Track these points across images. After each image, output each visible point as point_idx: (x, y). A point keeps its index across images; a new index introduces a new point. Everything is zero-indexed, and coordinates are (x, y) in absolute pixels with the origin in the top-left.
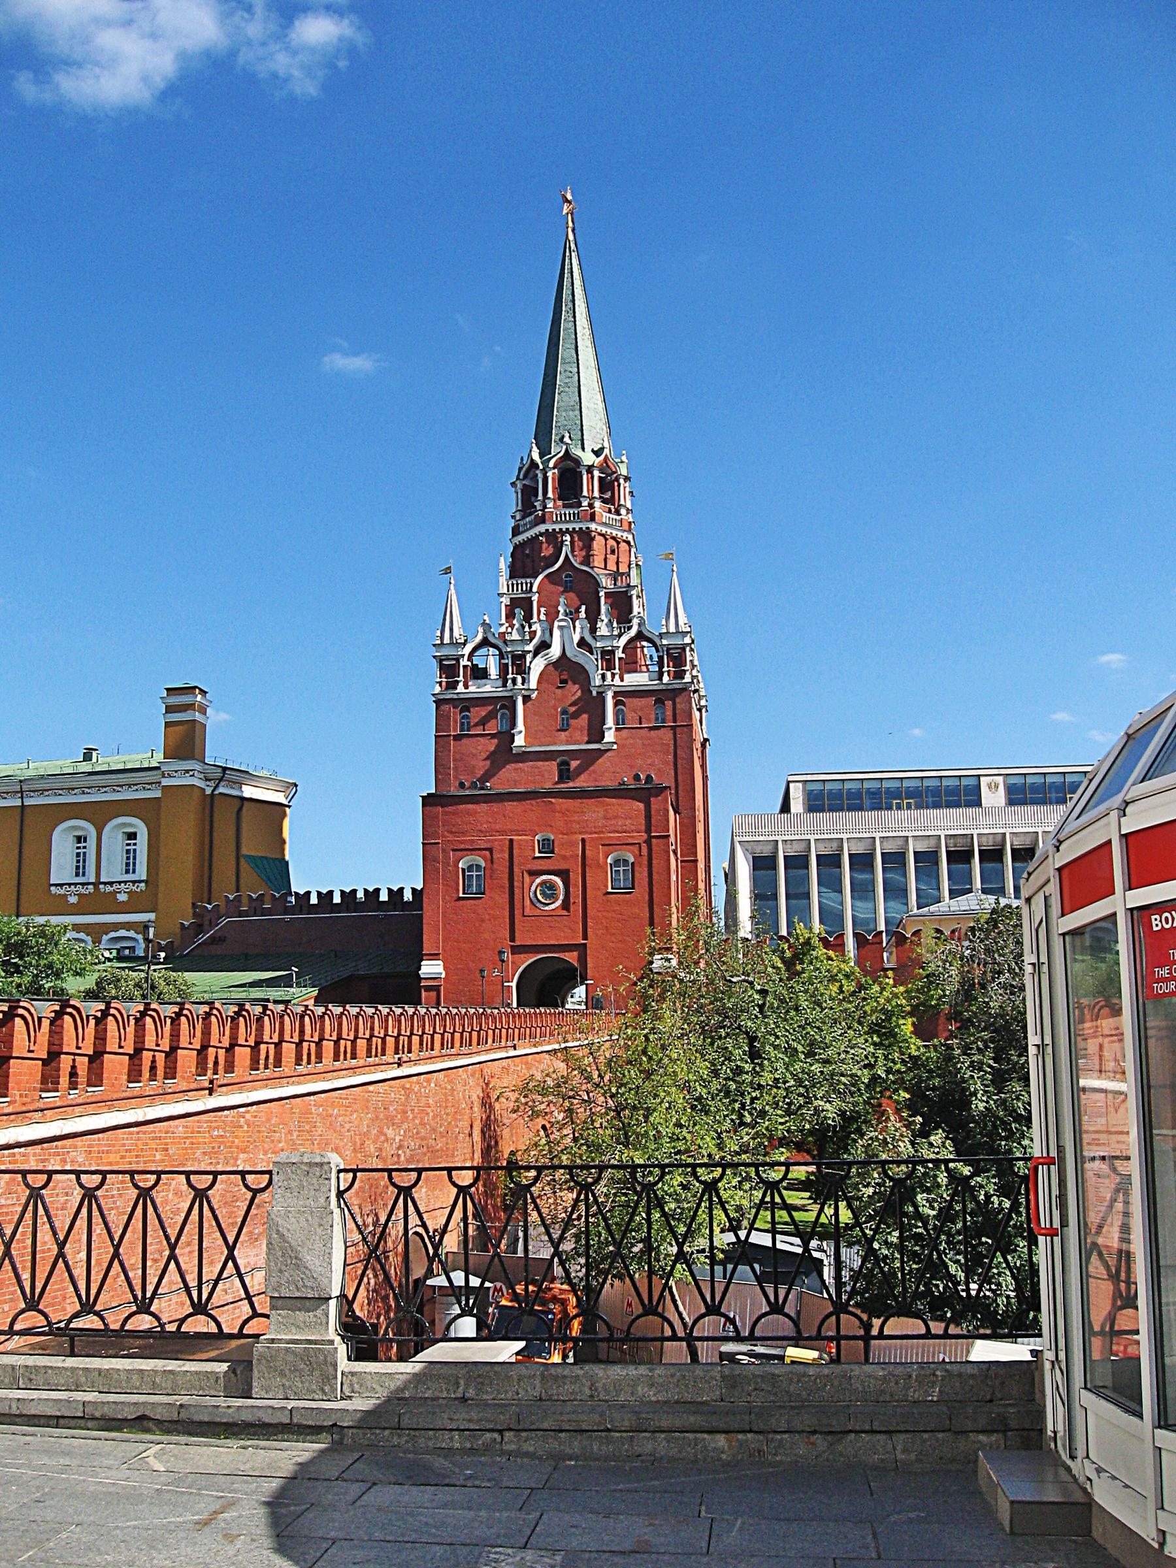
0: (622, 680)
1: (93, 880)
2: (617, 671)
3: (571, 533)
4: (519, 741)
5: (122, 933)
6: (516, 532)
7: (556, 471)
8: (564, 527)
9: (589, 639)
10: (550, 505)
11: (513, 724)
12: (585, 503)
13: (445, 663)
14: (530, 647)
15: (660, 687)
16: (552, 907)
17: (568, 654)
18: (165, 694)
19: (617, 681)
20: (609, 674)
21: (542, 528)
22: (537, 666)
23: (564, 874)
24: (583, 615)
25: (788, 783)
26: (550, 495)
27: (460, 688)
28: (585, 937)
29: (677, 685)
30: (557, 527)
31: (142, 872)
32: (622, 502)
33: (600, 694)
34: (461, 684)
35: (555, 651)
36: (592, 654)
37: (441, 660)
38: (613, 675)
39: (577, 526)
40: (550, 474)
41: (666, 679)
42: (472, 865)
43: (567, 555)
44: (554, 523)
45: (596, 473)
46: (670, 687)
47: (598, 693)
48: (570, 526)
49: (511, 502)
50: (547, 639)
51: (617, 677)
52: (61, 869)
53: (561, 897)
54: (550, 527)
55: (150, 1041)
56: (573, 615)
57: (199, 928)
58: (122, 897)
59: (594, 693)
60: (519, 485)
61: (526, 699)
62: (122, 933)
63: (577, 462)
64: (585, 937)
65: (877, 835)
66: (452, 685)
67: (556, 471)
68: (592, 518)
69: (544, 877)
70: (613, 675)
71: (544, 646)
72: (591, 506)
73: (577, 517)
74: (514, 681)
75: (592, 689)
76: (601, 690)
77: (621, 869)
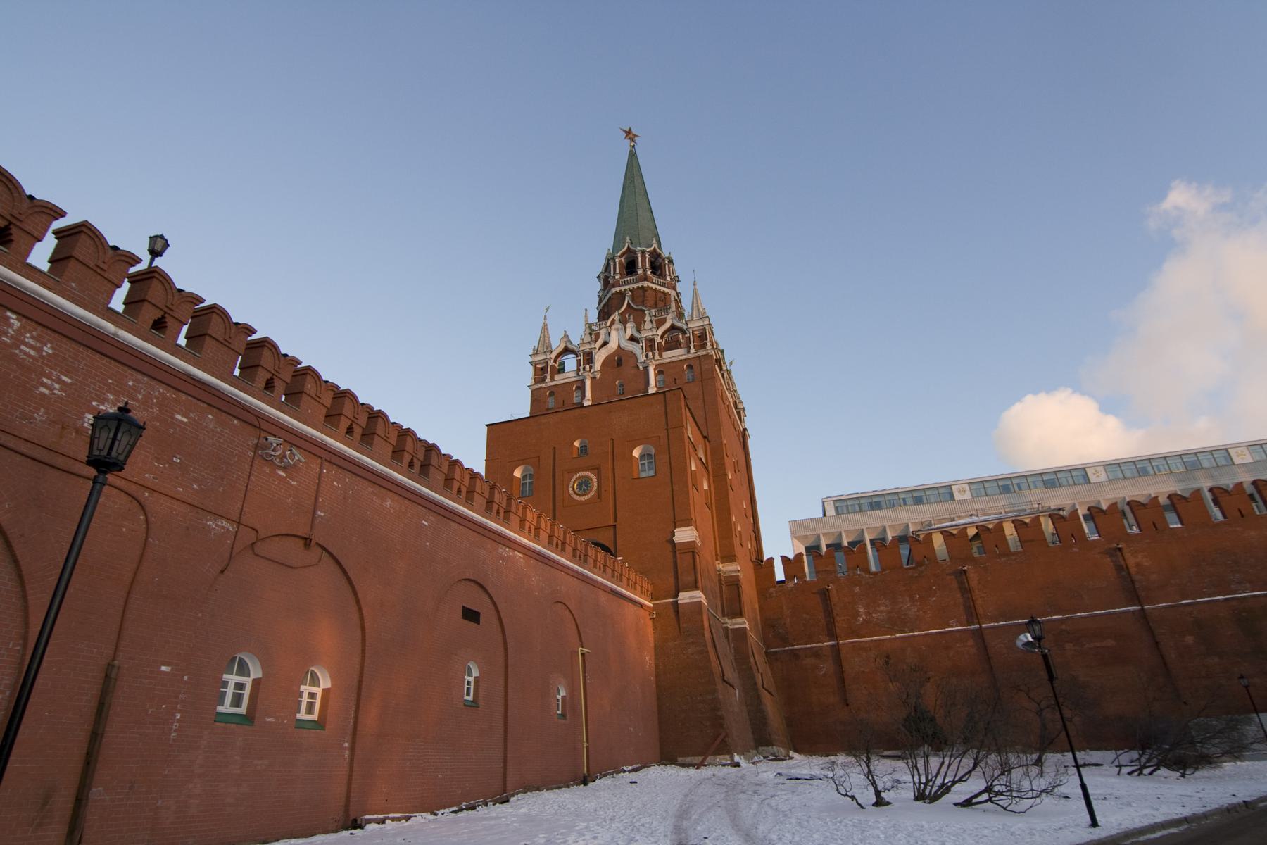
0: (661, 356)
2: (657, 352)
7: (623, 259)
9: (637, 335)
10: (617, 277)
12: (640, 272)
13: (538, 366)
16: (587, 497)
17: (622, 346)
19: (657, 357)
20: (650, 354)
21: (614, 290)
22: (599, 358)
23: (597, 470)
24: (632, 320)
25: (823, 503)
26: (618, 271)
27: (548, 379)
28: (615, 521)
29: (701, 353)
30: (622, 288)
32: (667, 272)
33: (646, 369)
34: (549, 377)
35: (613, 345)
36: (639, 343)
37: (536, 365)
38: (654, 355)
39: (635, 286)
40: (617, 260)
41: (692, 350)
42: (526, 475)
43: (628, 303)
44: (619, 286)
47: (644, 368)
48: (631, 287)
49: (598, 286)
50: (608, 341)
51: (657, 354)
53: (595, 488)
54: (618, 289)
56: (624, 322)
59: (641, 368)
60: (602, 277)
61: (593, 379)
63: (635, 252)
64: (615, 521)
65: (887, 524)
66: (543, 380)
67: (623, 259)
68: (645, 278)
69: (580, 474)
70: (654, 355)
71: (605, 344)
72: (645, 273)
73: (638, 281)
74: (584, 369)
75: (639, 365)
76: (645, 365)
77: (646, 462)
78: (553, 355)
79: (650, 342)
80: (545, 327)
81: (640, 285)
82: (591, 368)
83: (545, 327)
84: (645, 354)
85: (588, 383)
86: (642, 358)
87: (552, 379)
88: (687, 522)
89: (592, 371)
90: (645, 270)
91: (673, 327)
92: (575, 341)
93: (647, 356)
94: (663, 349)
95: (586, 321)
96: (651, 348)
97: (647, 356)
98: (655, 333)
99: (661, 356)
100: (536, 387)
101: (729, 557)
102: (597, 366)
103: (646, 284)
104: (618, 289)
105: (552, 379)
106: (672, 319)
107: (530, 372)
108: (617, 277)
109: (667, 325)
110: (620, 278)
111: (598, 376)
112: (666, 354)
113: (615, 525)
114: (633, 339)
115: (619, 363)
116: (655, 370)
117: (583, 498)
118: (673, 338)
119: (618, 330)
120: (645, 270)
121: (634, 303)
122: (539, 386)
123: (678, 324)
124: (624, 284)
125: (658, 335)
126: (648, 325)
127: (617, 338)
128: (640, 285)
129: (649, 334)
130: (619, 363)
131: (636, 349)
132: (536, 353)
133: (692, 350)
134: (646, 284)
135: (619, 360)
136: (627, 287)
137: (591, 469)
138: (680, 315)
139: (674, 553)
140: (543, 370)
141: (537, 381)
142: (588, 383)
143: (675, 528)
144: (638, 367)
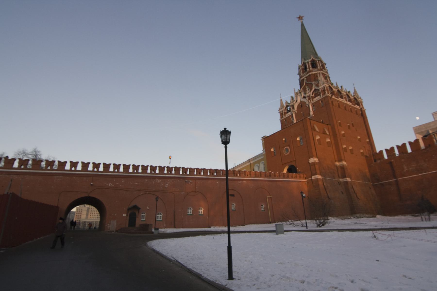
0: (313, 100)
2: (311, 100)
11: (293, 119)
14: (295, 102)
15: (321, 98)
19: (312, 101)
20: (309, 101)
23: (289, 146)
27: (284, 116)
29: (324, 96)
33: (309, 106)
35: (299, 101)
38: (310, 101)
39: (307, 75)
43: (306, 83)
45: (310, 63)
46: (323, 97)
53: (289, 151)
61: (295, 113)
64: (295, 159)
68: (310, 71)
69: (285, 148)
70: (310, 101)
74: (292, 110)
78: (284, 109)
79: (309, 96)
81: (308, 74)
82: (294, 110)
84: (308, 101)
85: (294, 115)
86: (307, 103)
88: (312, 157)
89: (295, 111)
91: (315, 90)
92: (289, 102)
93: (309, 102)
94: (313, 98)
95: (295, 92)
96: (309, 99)
97: (309, 102)
98: (310, 94)
99: (313, 100)
100: (281, 120)
102: (296, 109)
103: (310, 73)
105: (285, 116)
106: (314, 87)
107: (279, 115)
108: (302, 74)
109: (313, 89)
110: (303, 74)
111: (296, 112)
113: (295, 160)
114: (304, 97)
115: (302, 106)
116: (312, 105)
117: (287, 154)
118: (317, 93)
119: (299, 96)
120: (309, 68)
121: (307, 82)
122: (283, 119)
123: (317, 88)
124: (304, 76)
125: (311, 94)
126: (308, 91)
129: (308, 95)
131: (305, 100)
133: (322, 96)
134: (310, 73)
137: (288, 146)
139: (310, 165)
140: (282, 114)
142: (294, 115)
143: (310, 158)
144: (306, 106)
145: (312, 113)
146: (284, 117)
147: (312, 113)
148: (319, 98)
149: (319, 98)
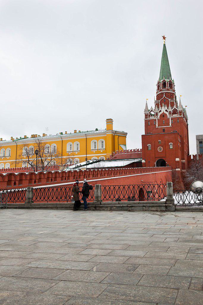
1: (97, 149)
3: (165, 93)
4: (157, 125)
5: (102, 157)
6: (157, 93)
8: (164, 92)
9: (167, 110)
12: (167, 88)
18: (106, 120)
21: (160, 92)
22: (159, 114)
27: (148, 118)
30: (163, 92)
31: (104, 148)
48: (165, 92)
49: (156, 88)
52: (92, 147)
54: (162, 92)
55: (102, 173)
57: (113, 156)
58: (102, 151)
61: (158, 119)
62: (102, 157)
71: (160, 111)
72: (168, 88)
80: (147, 103)
81: (167, 91)
83: (147, 103)
85: (157, 120)
87: (149, 118)
90: (168, 87)
98: (171, 110)
101: (184, 159)
102: (159, 117)
103: (168, 91)
104: (162, 92)
108: (162, 88)
109: (174, 108)
110: (162, 89)
112: (173, 115)
114: (166, 111)
118: (175, 112)
120: (168, 87)
124: (163, 90)
127: (163, 109)
128: (167, 91)
130: (163, 116)
131: (167, 113)
132: (145, 111)
133: (179, 115)
134: (168, 91)
135: (163, 115)
136: (164, 92)
138: (177, 107)
141: (146, 118)
142: (157, 120)
145: (170, 125)
146: (148, 119)
147: (170, 125)
148: (177, 116)
149: (177, 116)
